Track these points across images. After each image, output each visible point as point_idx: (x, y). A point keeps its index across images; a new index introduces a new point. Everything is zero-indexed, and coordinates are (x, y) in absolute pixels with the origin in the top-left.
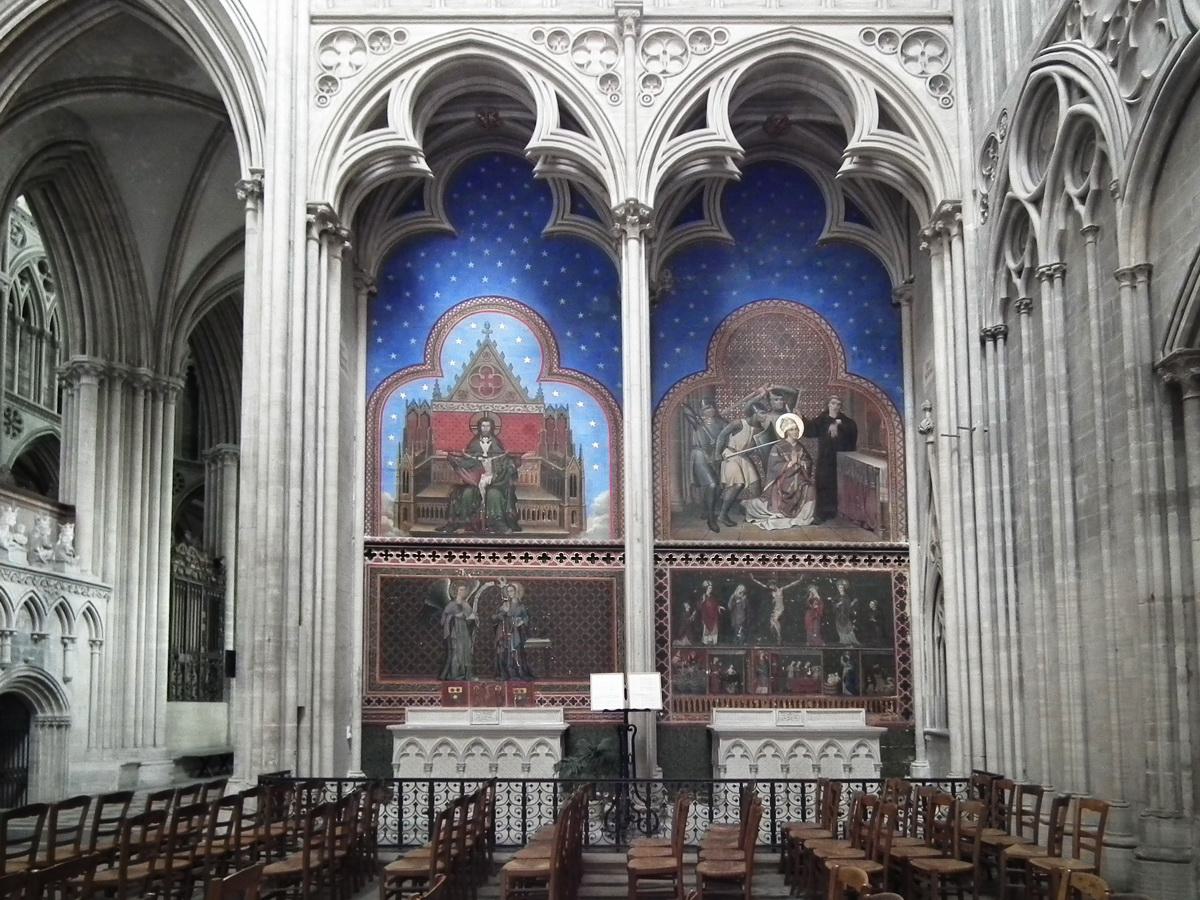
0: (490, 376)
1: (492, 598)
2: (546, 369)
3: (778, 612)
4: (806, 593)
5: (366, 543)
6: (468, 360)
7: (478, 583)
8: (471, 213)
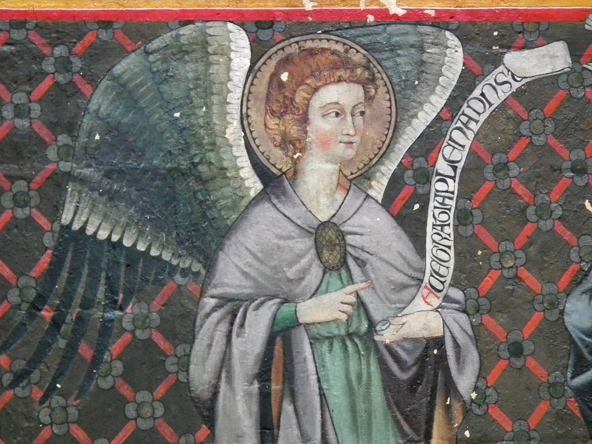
7: (454, 58)
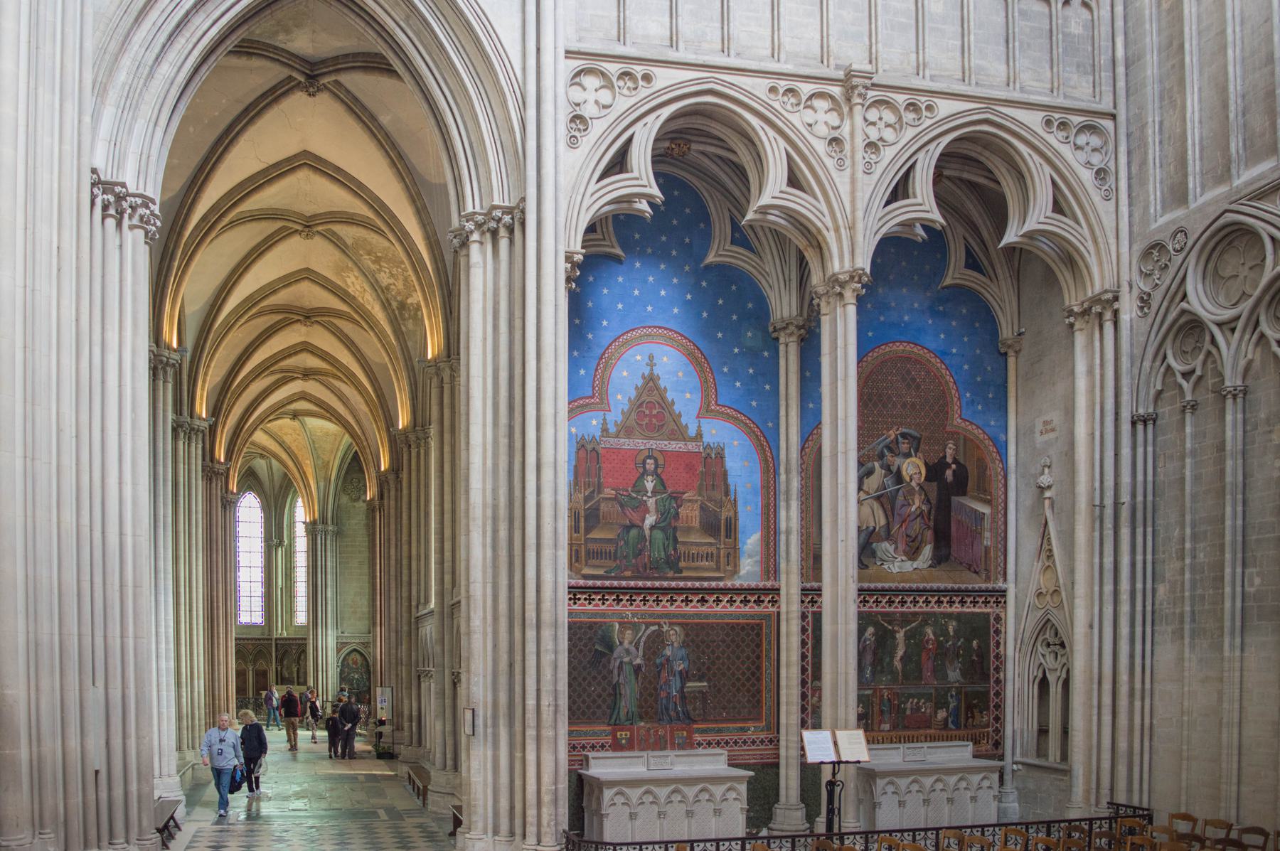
0: (655, 412)
1: (657, 642)
3: (900, 652)
4: (923, 634)
6: (633, 394)
8: (637, 236)
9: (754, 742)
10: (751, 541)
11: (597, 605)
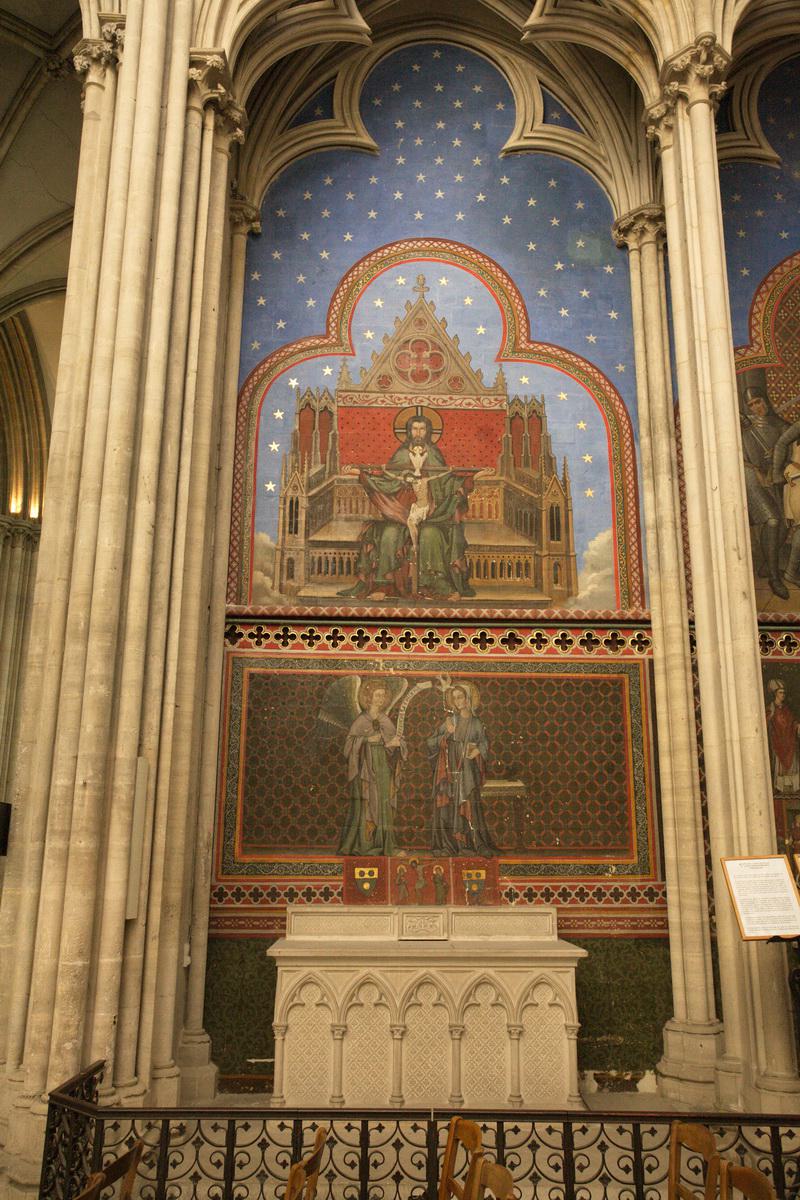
0: (426, 354)
1: (427, 711)
2: (509, 345)
5: (229, 616)
6: (391, 328)
7: (406, 683)
8: (400, 124)
9: (617, 895)
10: (596, 544)
11: (324, 647)
